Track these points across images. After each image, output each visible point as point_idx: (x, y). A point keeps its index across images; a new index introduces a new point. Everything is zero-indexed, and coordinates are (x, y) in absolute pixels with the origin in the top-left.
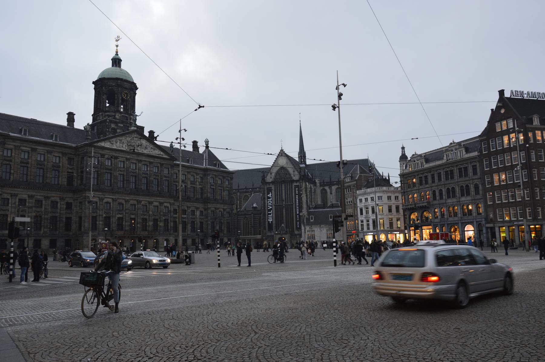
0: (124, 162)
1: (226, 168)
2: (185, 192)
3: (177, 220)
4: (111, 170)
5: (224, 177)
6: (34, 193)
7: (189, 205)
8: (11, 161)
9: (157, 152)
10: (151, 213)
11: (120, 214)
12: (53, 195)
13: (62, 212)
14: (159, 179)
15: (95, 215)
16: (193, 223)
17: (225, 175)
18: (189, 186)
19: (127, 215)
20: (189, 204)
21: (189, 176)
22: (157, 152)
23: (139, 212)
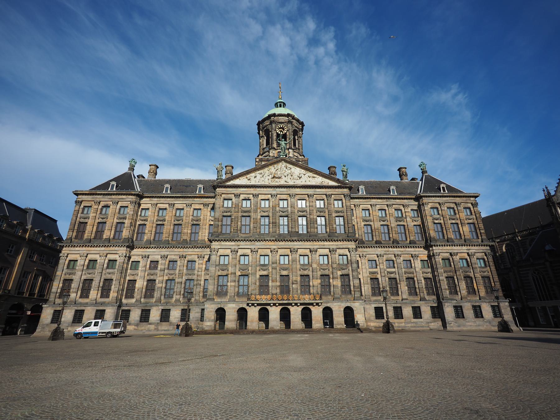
0: (268, 200)
3: (379, 276)
6: (168, 253)
7: (396, 253)
10: (315, 266)
11: (264, 270)
12: (189, 253)
13: (199, 273)
14: (327, 216)
18: (393, 225)
19: (274, 271)
22: (318, 180)
23: (294, 266)
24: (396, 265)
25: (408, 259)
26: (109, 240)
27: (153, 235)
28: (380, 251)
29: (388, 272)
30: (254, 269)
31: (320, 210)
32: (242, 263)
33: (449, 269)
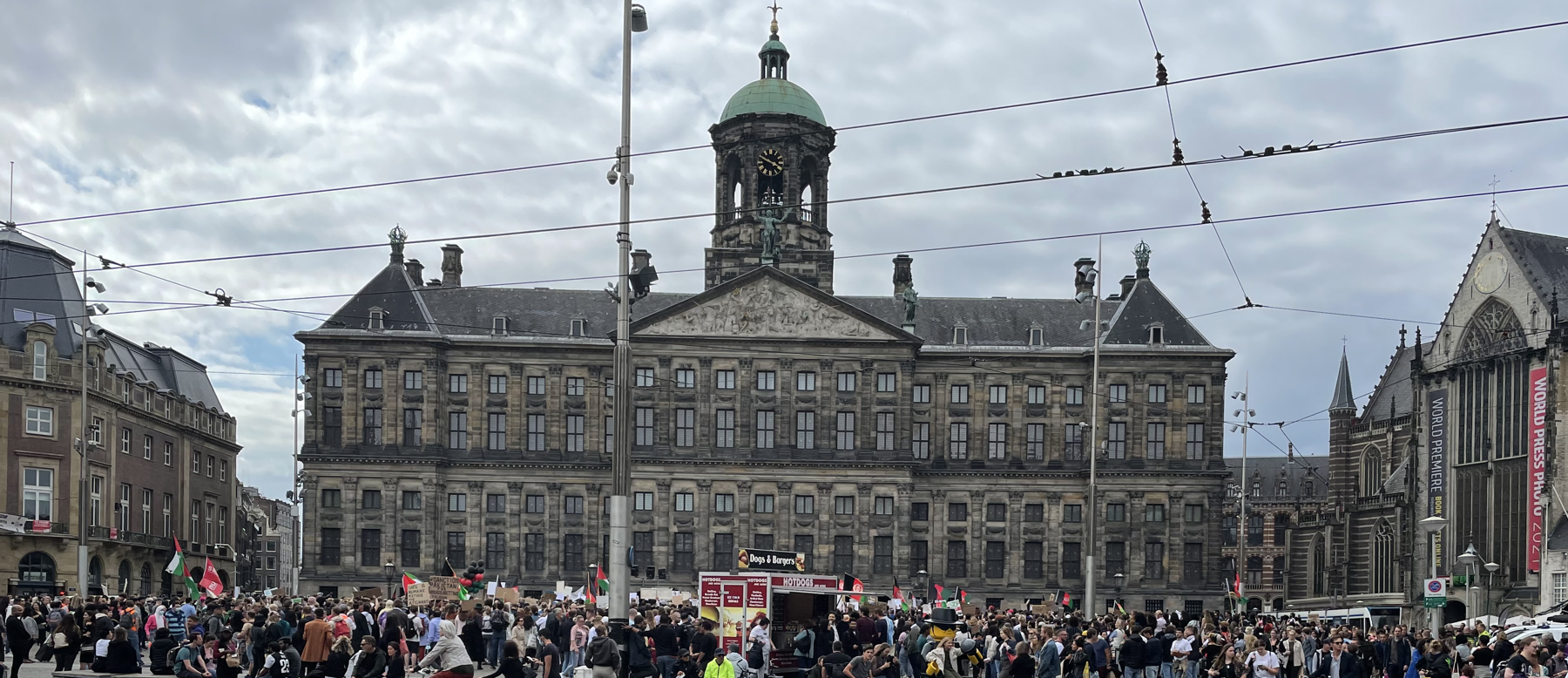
1: (1200, 340)
2: (1006, 443)
3: (967, 538)
4: (691, 399)
5: (1177, 378)
7: (1014, 488)
8: (465, 403)
9: (846, 327)
10: (824, 518)
15: (646, 527)
16: (1034, 546)
17: (1180, 367)
19: (744, 527)
20: (1014, 484)
21: (1018, 389)
22: (846, 327)
23: (784, 517)
24: (1008, 515)
25: (1037, 501)
26: (393, 447)
27: (484, 438)
28: (977, 484)
29: (989, 529)
30: (704, 521)
31: (847, 398)
32: (680, 507)
33: (1116, 525)
